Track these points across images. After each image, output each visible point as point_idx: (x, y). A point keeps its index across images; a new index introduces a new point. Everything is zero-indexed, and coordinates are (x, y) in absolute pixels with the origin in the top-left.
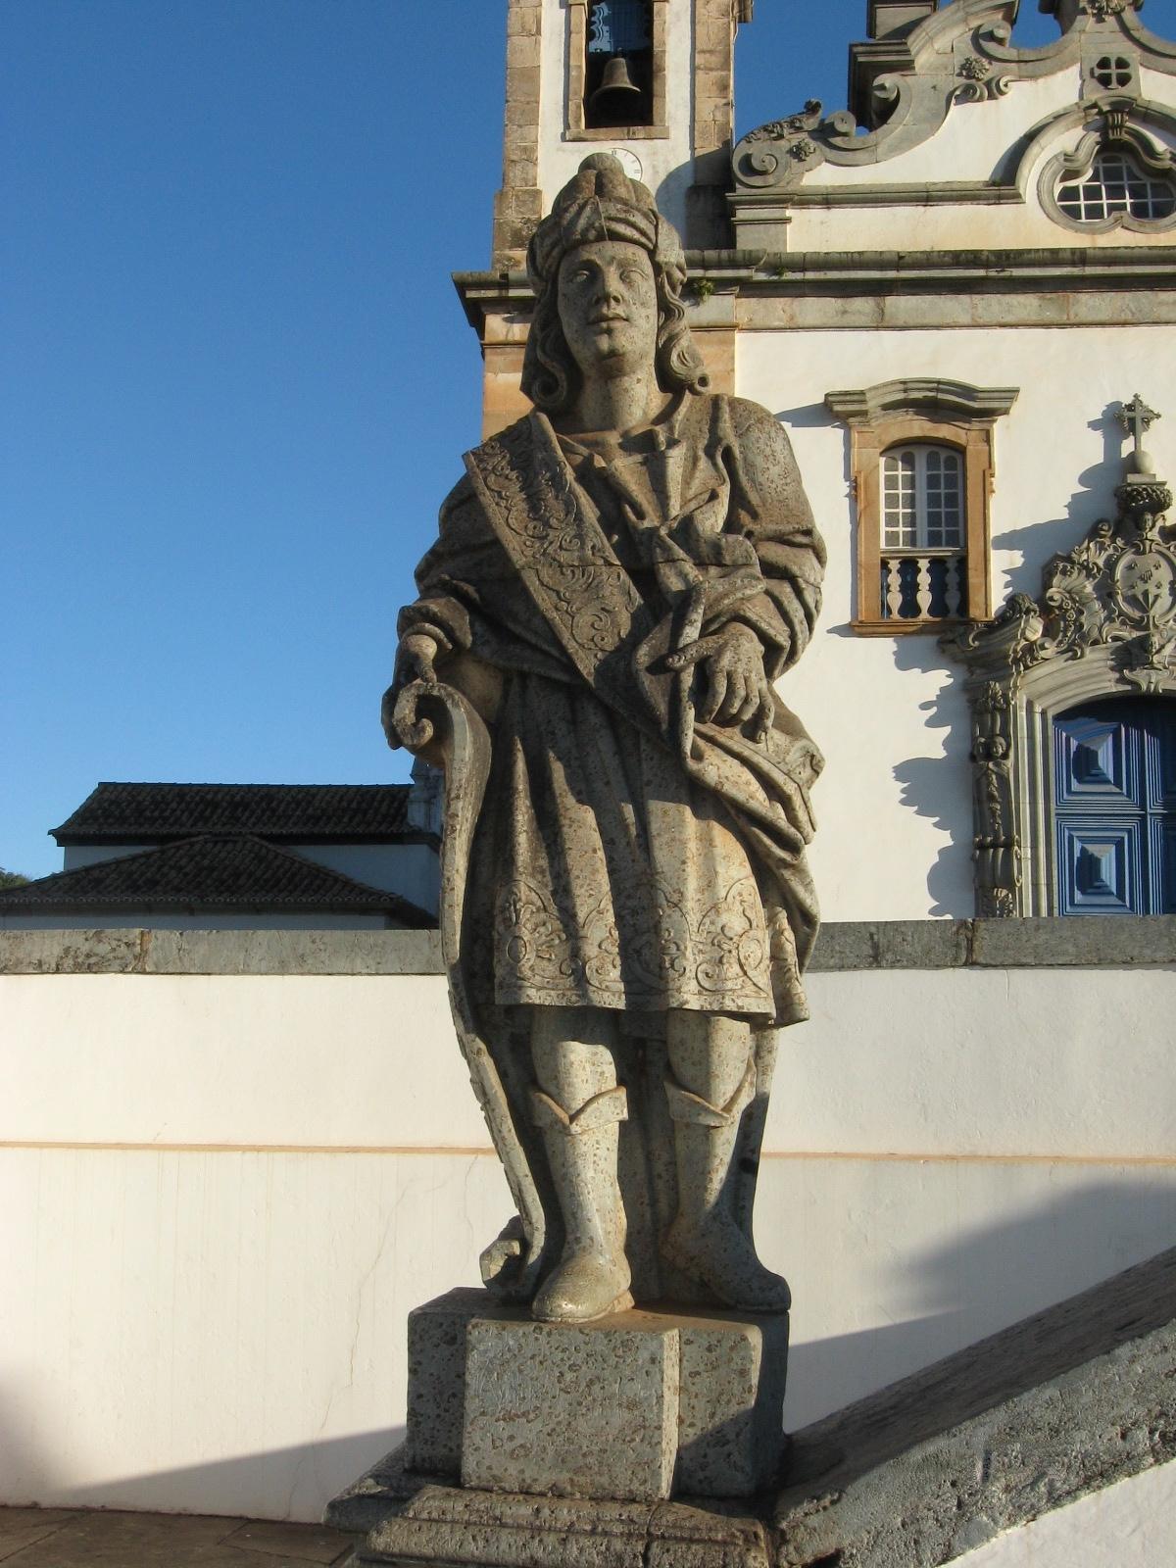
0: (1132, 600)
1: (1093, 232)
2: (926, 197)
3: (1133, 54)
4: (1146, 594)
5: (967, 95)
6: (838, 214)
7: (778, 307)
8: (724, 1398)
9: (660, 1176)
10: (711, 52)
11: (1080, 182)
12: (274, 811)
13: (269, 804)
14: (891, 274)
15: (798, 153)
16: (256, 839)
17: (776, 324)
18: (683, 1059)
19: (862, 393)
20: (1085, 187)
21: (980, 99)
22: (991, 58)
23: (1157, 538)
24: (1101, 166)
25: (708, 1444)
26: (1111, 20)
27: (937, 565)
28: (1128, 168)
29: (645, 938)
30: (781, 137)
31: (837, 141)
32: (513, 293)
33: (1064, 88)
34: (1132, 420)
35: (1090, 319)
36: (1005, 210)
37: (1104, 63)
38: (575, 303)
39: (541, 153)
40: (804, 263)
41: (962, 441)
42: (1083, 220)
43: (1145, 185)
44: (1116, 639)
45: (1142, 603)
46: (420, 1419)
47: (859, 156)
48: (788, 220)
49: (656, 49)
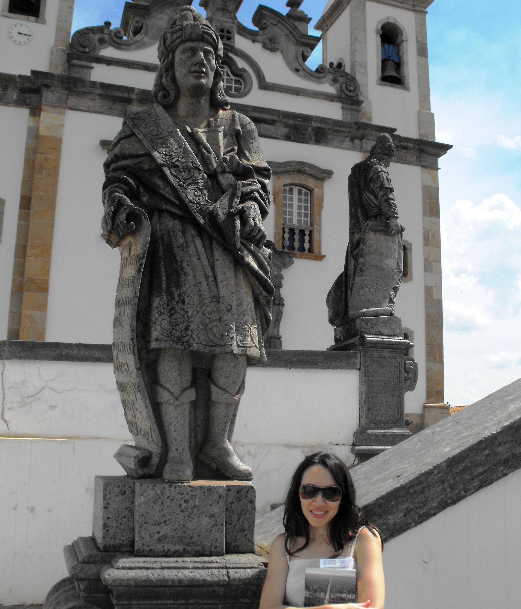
8: (244, 512)
9: (198, 426)
17: (83, 109)
18: (221, 375)
25: (237, 532)
28: (227, 72)
29: (214, 324)
37: (222, 31)
38: (185, 63)
43: (232, 79)
46: (108, 528)
47: (124, 47)
48: (92, 68)
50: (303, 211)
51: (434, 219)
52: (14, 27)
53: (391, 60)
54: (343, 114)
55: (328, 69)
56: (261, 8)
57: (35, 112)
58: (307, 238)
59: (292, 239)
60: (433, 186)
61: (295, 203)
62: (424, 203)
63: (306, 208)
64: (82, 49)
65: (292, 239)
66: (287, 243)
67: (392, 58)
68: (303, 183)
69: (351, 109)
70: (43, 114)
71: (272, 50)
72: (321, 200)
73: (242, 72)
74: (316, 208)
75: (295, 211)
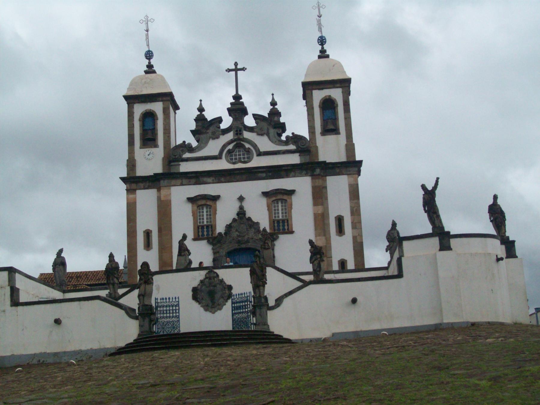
1: (234, 163)
12: (88, 278)
15: (182, 151)
16: (84, 286)
17: (178, 184)
20: (234, 154)
24: (237, 150)
33: (230, 136)
37: (237, 131)
41: (211, 204)
44: (237, 239)
48: (180, 165)
50: (284, 211)
51: (356, 201)
52: (146, 152)
53: (330, 119)
54: (300, 158)
55: (291, 137)
56: (254, 115)
57: (159, 190)
58: (286, 224)
59: (278, 226)
60: (355, 183)
61: (280, 208)
63: (286, 209)
64: (174, 157)
65: (278, 226)
66: (276, 228)
67: (331, 118)
70: (162, 190)
71: (262, 135)
72: (291, 205)
75: (280, 212)
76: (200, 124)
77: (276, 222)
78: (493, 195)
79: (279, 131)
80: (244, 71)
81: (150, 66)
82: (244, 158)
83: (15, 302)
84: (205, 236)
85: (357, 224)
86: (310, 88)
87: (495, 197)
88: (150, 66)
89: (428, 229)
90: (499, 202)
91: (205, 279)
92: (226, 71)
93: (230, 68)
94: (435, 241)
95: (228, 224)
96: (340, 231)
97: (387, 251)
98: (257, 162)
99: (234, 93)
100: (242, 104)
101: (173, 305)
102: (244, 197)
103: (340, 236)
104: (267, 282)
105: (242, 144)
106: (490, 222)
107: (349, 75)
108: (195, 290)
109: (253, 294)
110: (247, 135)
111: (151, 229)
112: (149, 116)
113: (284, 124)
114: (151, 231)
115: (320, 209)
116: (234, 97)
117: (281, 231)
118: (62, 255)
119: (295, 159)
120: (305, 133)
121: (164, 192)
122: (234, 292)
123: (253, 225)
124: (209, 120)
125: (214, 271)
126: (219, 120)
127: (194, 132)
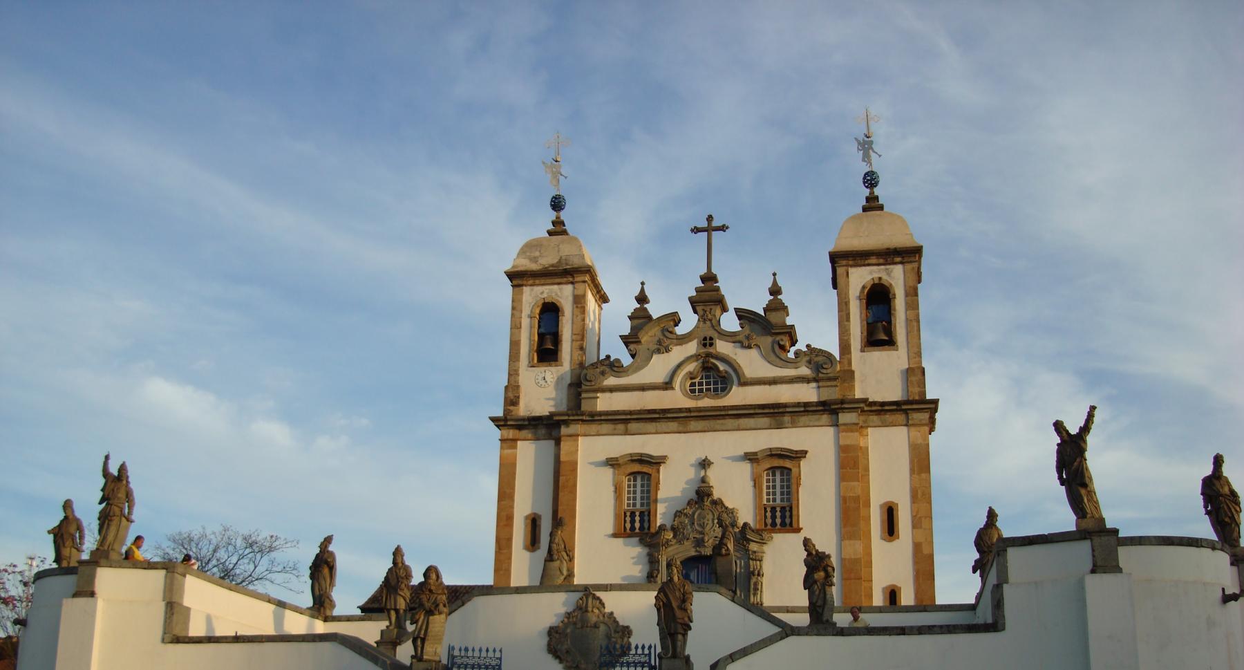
0: (700, 525)
1: (697, 398)
2: (643, 388)
3: (715, 335)
4: (704, 523)
5: (659, 351)
6: (615, 395)
7: (594, 428)
10: (578, 334)
11: (697, 380)
13: (455, 594)
14: (629, 417)
15: (603, 373)
17: (592, 434)
19: (617, 458)
21: (663, 353)
22: (667, 337)
23: (709, 505)
26: (708, 323)
27: (642, 514)
30: (597, 367)
31: (615, 369)
32: (509, 423)
34: (704, 464)
35: (695, 430)
36: (669, 392)
37: (705, 339)
39: (520, 372)
40: (601, 414)
42: (697, 394)
44: (694, 538)
45: (702, 526)
47: (624, 374)
48: (598, 397)
49: (560, 333)
51: (924, 475)
56: (737, 310)
58: (788, 514)
59: (774, 517)
62: (912, 462)
65: (774, 517)
66: (769, 521)
68: (782, 465)
69: (828, 386)
70: (562, 443)
71: (749, 347)
73: (724, 374)
74: (794, 487)
76: (637, 322)
77: (769, 509)
78: (1214, 455)
79: (782, 340)
80: (725, 231)
81: (558, 223)
82: (716, 390)
83: (176, 636)
84: (637, 531)
85: (922, 520)
86: (844, 262)
87: (1218, 461)
88: (558, 223)
89: (1066, 520)
90: (1226, 471)
91: (574, 611)
92: (692, 231)
93: (699, 226)
94: (1083, 549)
95: (679, 509)
96: (891, 529)
97: (974, 571)
98: (738, 396)
99: (704, 271)
100: (718, 289)
101: (488, 664)
102: (712, 461)
103: (890, 541)
104: (691, 624)
105: (714, 364)
106: (1206, 514)
107: (918, 241)
108: (552, 631)
109: (659, 650)
110: (722, 347)
111: (540, 513)
112: (550, 311)
113: (792, 327)
114: (540, 517)
115: (857, 487)
116: (704, 279)
117: (778, 526)
118: (331, 548)
119: (808, 393)
120: (832, 346)
121: (565, 446)
122: (634, 641)
123: (724, 516)
124: (655, 317)
125: (594, 595)
126: (674, 319)
127: (628, 340)
